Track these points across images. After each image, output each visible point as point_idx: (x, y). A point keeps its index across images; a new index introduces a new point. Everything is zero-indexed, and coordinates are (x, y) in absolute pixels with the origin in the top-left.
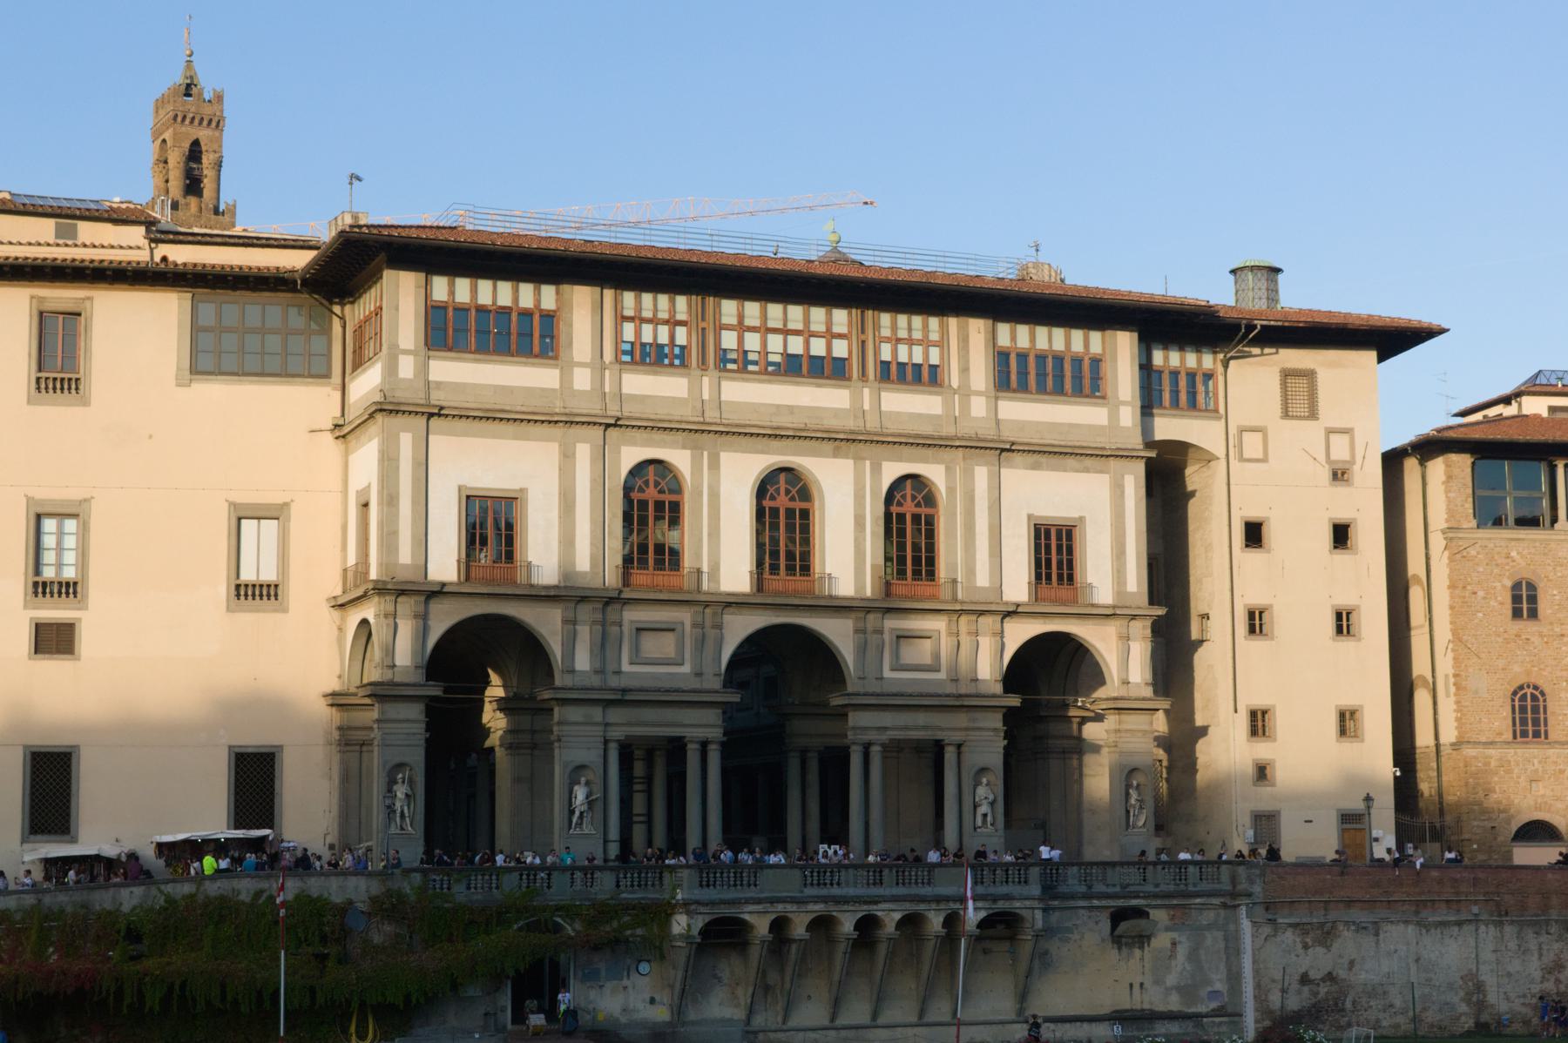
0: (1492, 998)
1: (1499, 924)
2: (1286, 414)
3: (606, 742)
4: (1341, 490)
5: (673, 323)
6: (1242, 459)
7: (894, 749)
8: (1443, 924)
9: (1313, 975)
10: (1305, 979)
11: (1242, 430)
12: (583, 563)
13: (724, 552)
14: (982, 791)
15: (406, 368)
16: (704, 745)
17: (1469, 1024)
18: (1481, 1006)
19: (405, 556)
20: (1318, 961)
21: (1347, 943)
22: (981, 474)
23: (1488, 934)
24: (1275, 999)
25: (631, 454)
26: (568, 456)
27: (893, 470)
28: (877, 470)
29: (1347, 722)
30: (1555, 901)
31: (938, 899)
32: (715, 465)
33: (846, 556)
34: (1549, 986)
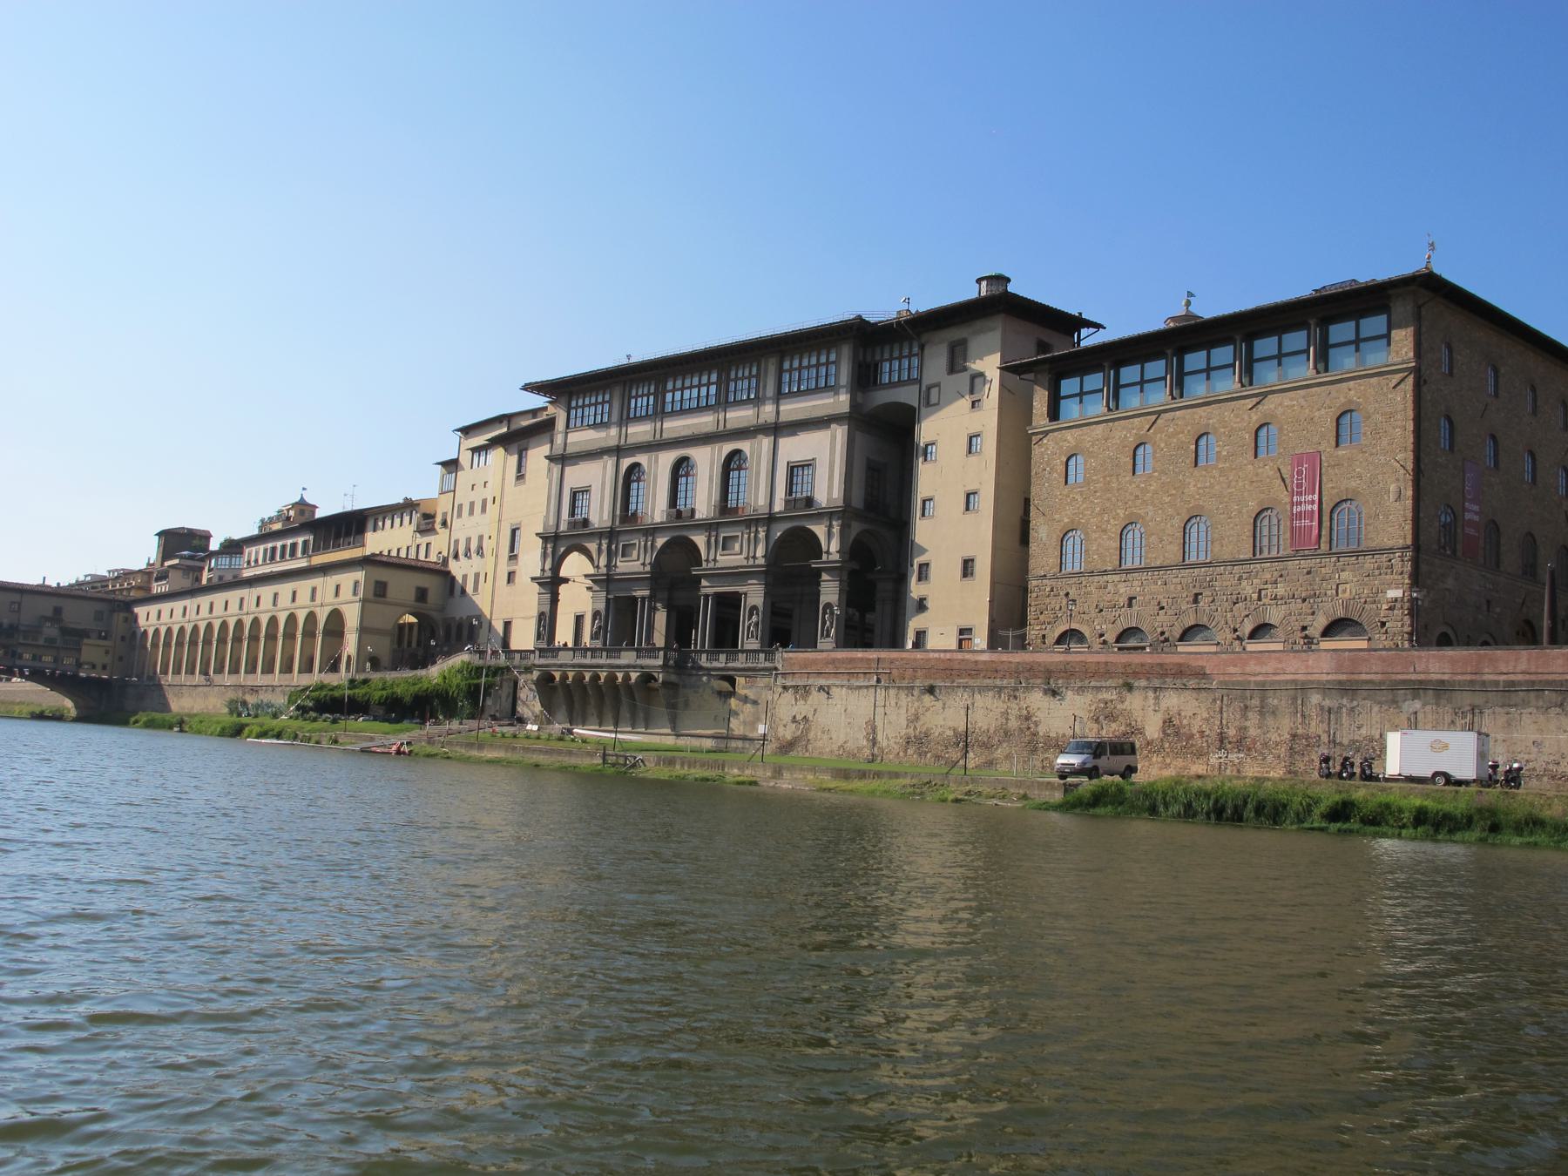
0: (879, 738)
1: (887, 688)
2: (952, 369)
3: (608, 600)
4: (977, 414)
5: (648, 396)
6: (928, 404)
7: (717, 595)
8: (860, 687)
9: (799, 718)
10: (794, 720)
11: (929, 388)
12: (606, 516)
13: (654, 505)
14: (754, 618)
15: (559, 439)
16: (643, 598)
17: (867, 752)
18: (874, 742)
19: (552, 521)
20: (802, 709)
21: (816, 697)
22: (766, 442)
23: (881, 693)
24: (781, 731)
25: (626, 463)
26: (605, 467)
27: (728, 447)
28: (720, 450)
29: (968, 567)
30: (919, 673)
31: (619, 667)
32: (657, 461)
33: (703, 499)
34: (911, 731)
